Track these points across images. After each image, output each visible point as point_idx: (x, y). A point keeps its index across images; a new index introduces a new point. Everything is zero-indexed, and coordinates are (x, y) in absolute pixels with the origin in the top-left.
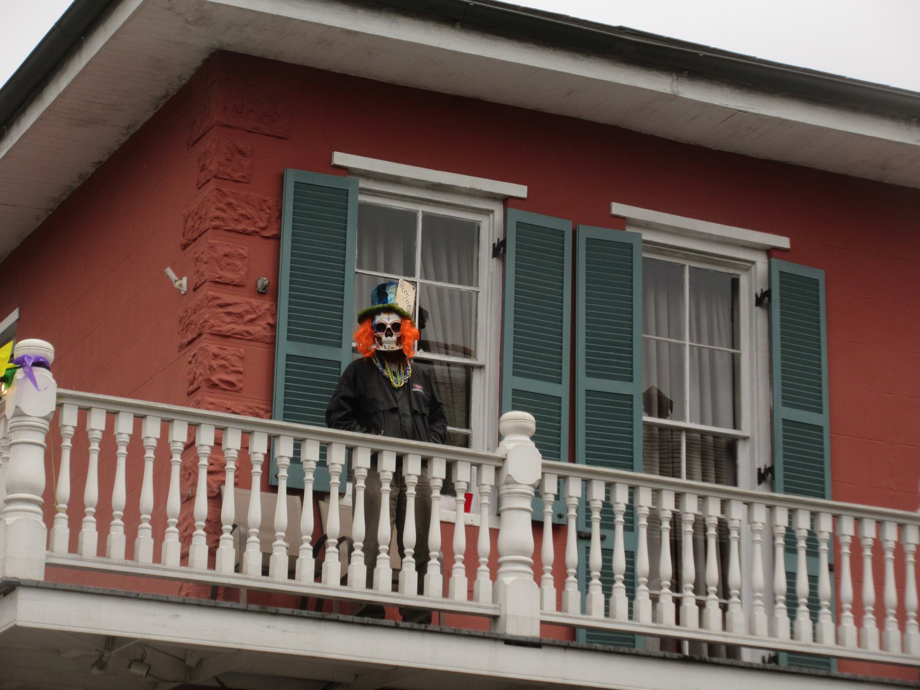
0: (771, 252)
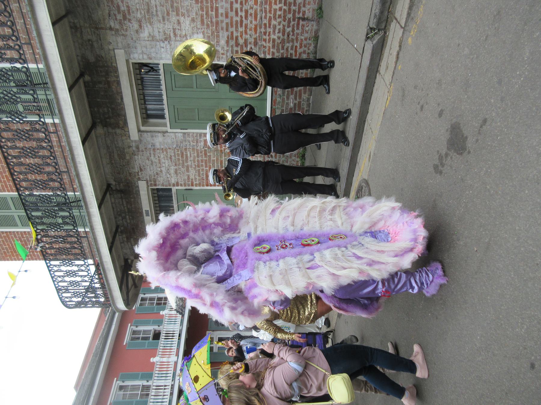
0: (117, 381)
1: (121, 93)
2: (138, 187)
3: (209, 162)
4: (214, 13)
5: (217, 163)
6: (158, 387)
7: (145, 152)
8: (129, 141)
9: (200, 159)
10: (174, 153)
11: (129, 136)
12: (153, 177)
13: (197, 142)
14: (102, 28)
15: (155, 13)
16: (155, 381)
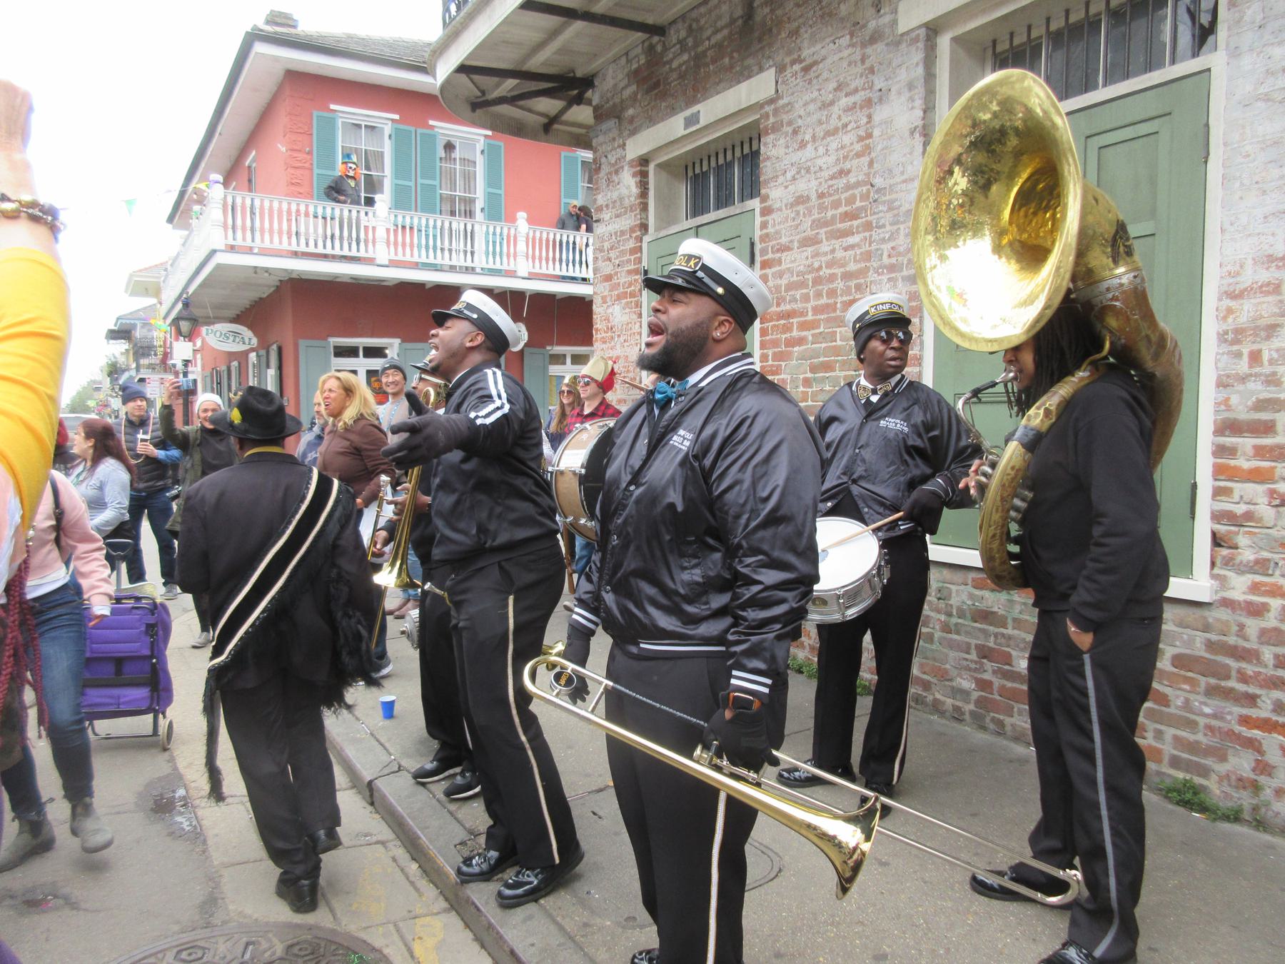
0: (486, 136)
2: (761, 70)
3: (828, 320)
5: (826, 352)
6: (470, 236)
7: (860, 68)
9: (839, 284)
10: (858, 184)
12: (785, 118)
13: (892, 268)
16: (484, 228)
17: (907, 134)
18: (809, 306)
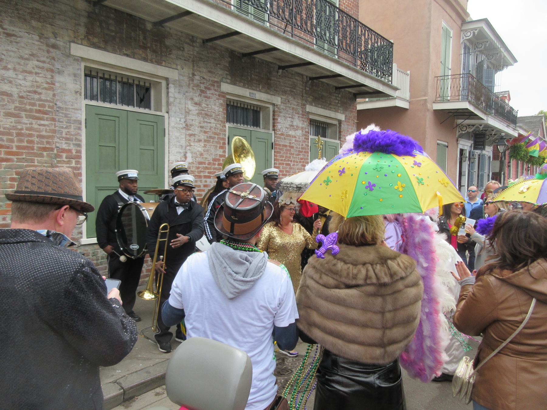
1: (134, 58)
3: (28, 153)
4: (207, 174)
7: (46, 54)
8: (67, 38)
9: (36, 139)
10: (47, 101)
11: (74, 42)
13: (67, 139)
14: (193, 66)
15: (206, 120)
17: (73, 92)
18: (14, 145)
